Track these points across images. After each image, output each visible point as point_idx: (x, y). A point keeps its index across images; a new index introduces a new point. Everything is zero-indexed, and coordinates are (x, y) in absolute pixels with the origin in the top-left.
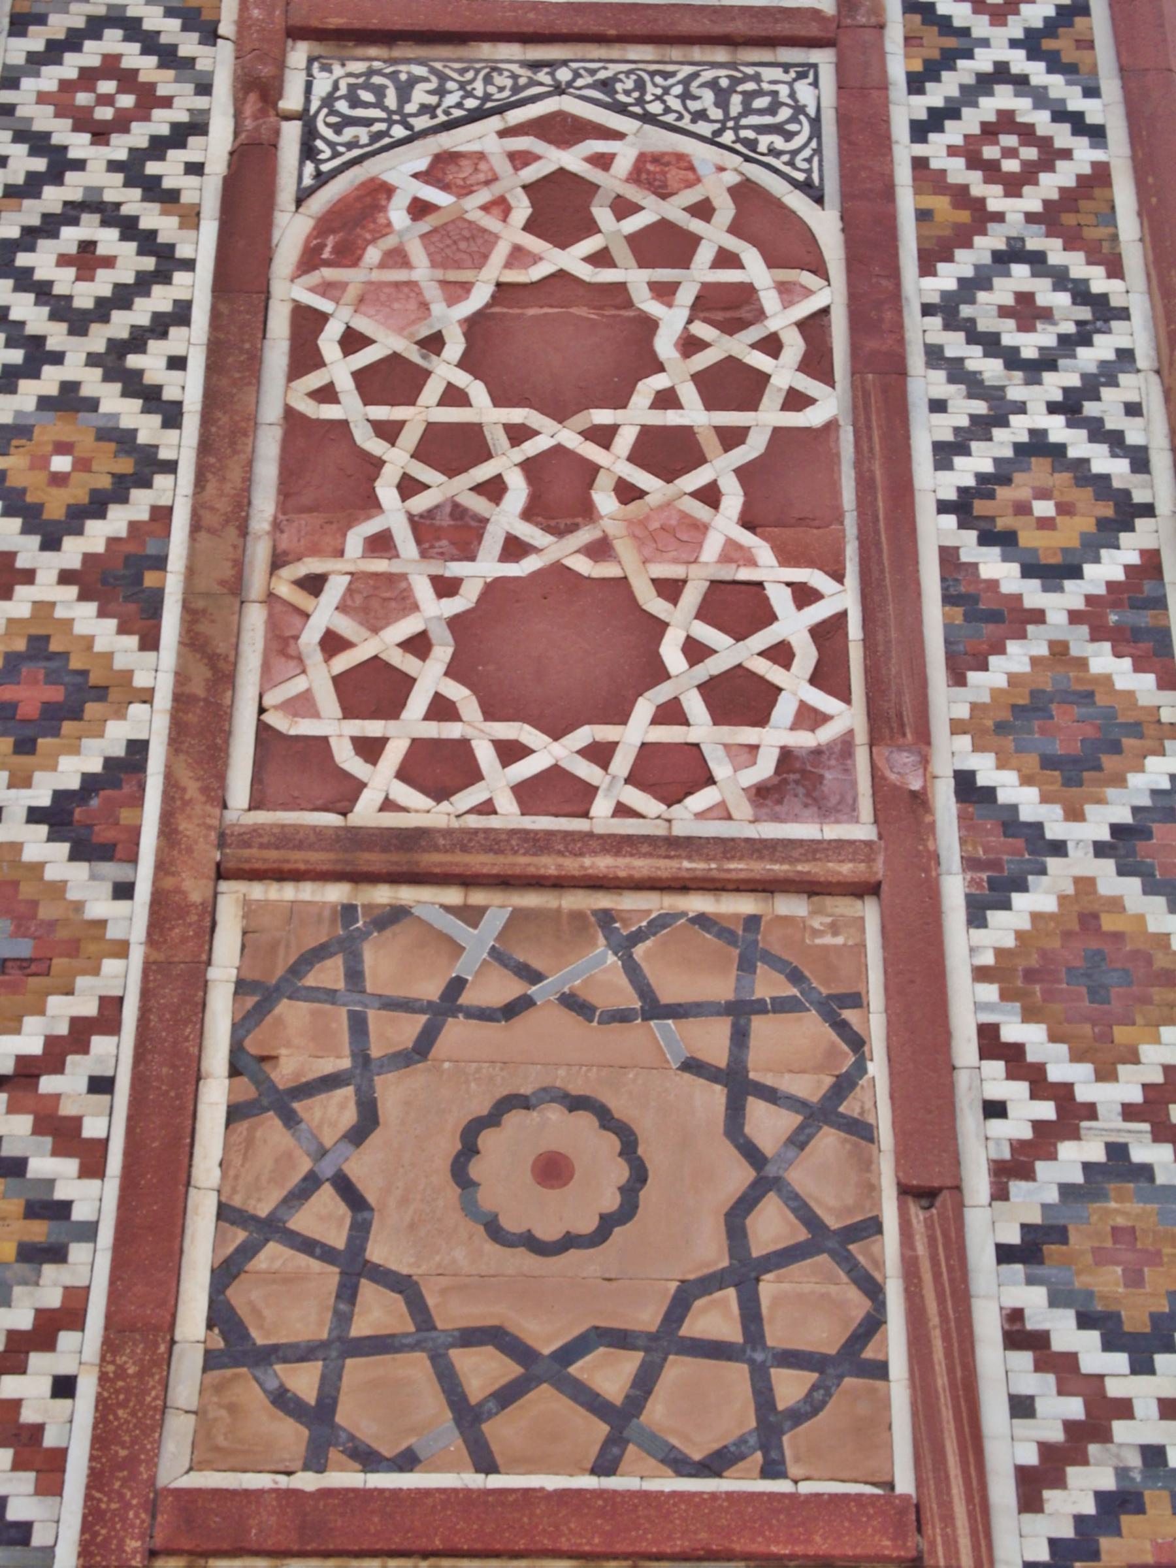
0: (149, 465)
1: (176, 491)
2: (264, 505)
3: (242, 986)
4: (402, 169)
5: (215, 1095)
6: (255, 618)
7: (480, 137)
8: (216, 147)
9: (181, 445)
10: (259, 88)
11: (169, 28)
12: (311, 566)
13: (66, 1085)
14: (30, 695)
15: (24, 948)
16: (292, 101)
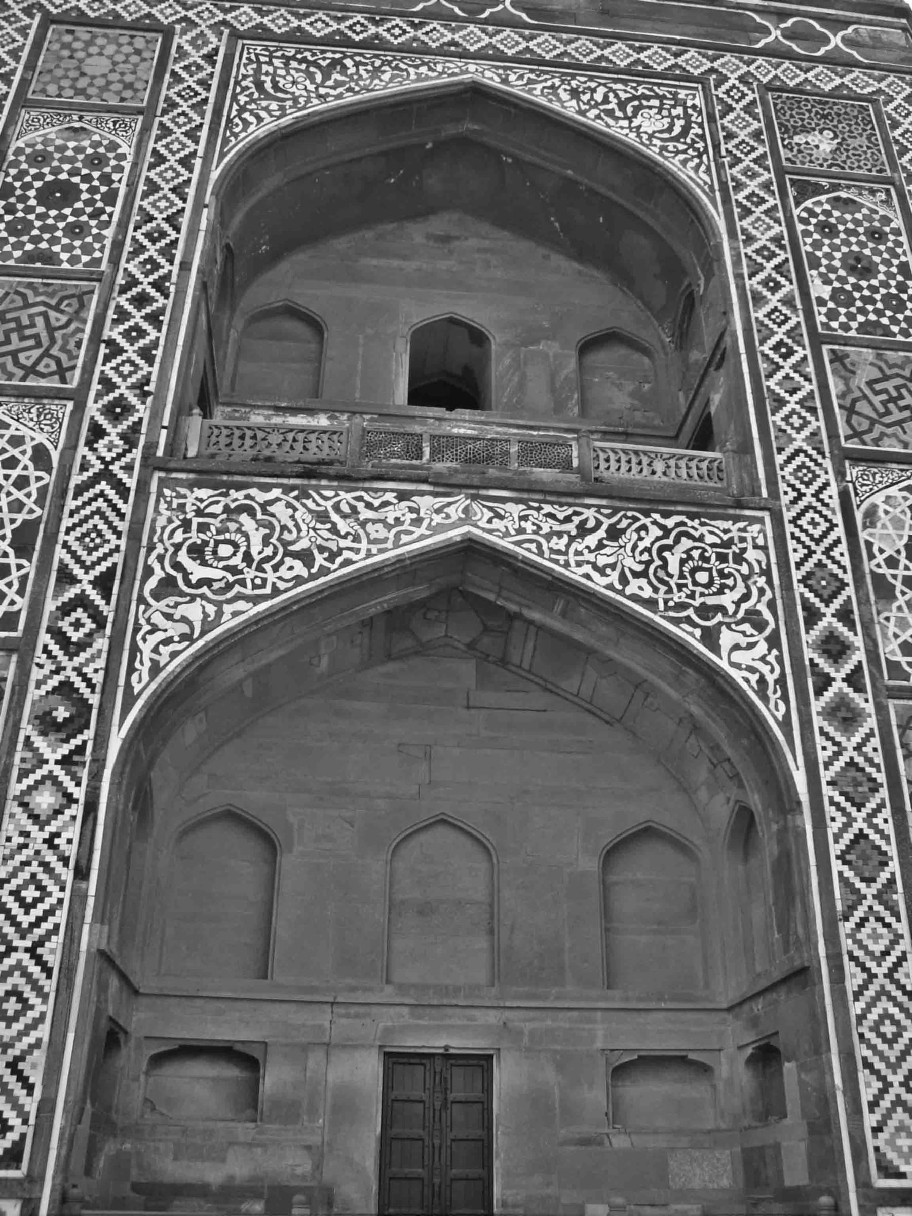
0: (843, 585)
1: (850, 591)
2: (872, 598)
3: (899, 726)
4: (878, 499)
5: (900, 753)
6: (877, 627)
7: (893, 491)
8: (833, 490)
9: (848, 578)
10: (840, 474)
11: (814, 453)
12: (886, 614)
13: (868, 749)
14: (835, 648)
15: (849, 715)
16: (848, 478)
